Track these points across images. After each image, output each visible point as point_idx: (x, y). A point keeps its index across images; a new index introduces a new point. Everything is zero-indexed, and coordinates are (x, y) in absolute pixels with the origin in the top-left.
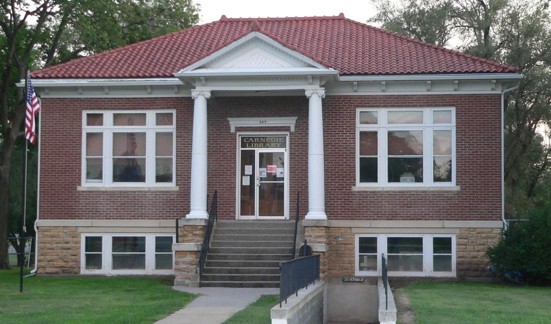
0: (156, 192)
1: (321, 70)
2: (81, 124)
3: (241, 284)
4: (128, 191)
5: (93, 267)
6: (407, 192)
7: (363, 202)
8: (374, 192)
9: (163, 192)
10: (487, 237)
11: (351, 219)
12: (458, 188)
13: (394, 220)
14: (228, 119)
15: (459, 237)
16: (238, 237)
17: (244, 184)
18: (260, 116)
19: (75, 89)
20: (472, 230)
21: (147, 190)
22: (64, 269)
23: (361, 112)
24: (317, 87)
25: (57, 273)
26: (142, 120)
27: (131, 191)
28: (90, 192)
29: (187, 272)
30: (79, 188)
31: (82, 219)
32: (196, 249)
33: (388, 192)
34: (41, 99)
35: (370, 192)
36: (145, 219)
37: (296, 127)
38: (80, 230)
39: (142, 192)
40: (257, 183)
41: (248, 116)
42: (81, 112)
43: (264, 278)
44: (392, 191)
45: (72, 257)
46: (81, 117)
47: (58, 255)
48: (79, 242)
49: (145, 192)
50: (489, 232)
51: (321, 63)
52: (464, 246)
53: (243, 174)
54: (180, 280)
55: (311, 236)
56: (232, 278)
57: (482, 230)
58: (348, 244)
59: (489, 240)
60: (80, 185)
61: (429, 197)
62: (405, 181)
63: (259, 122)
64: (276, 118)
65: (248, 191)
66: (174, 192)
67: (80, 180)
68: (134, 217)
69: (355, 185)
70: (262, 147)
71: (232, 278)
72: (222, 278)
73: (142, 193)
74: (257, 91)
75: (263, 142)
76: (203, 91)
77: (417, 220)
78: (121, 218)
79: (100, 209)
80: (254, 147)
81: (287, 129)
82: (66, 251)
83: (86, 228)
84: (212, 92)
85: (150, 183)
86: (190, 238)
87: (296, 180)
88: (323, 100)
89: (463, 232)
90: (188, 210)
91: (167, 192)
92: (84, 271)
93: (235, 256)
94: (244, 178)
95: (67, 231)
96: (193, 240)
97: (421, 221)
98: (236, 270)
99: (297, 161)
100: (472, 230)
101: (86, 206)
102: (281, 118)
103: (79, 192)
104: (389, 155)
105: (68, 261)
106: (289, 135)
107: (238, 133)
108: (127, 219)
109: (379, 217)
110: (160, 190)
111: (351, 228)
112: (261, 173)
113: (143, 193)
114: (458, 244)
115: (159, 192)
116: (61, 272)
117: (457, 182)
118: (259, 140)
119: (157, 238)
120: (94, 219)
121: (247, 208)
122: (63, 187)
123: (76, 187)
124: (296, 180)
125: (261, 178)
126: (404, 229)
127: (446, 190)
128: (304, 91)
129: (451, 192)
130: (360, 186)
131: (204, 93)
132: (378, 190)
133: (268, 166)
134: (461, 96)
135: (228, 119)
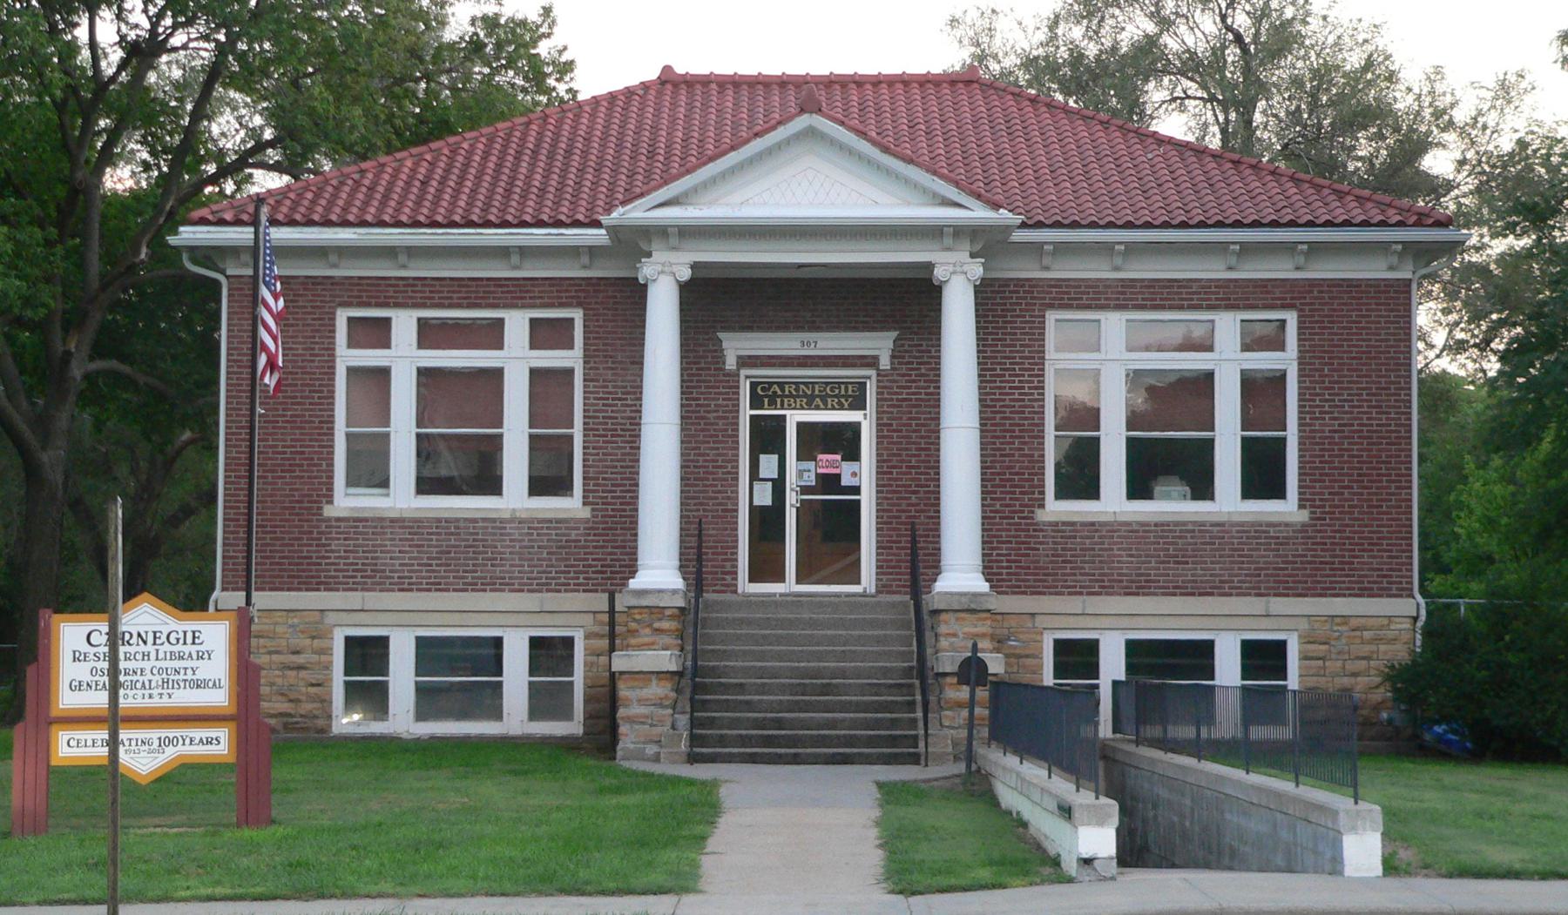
0: (532, 520)
1: (979, 213)
4: (457, 520)
6: (1177, 524)
8: (1093, 524)
9: (550, 521)
10: (1377, 640)
11: (1033, 593)
13: (1144, 594)
14: (721, 335)
15: (1307, 639)
16: (764, 636)
17: (756, 503)
18: (799, 328)
20: (1338, 620)
21: (507, 516)
23: (1057, 320)
24: (964, 256)
30: (329, 511)
32: (673, 668)
34: (227, 277)
35: (1083, 524)
37: (893, 357)
38: (331, 618)
39: (494, 520)
40: (791, 499)
43: (850, 741)
44: (1138, 523)
45: (312, 690)
48: (327, 651)
49: (502, 521)
50: (1381, 628)
51: (979, 197)
53: (754, 475)
55: (955, 635)
56: (769, 741)
57: (1363, 621)
58: (1027, 656)
59: (1383, 648)
60: (331, 502)
62: (1167, 497)
63: (798, 345)
65: (767, 522)
67: (331, 490)
69: (1042, 506)
71: (769, 741)
72: (744, 741)
73: (495, 524)
75: (805, 395)
76: (671, 264)
77: (1201, 594)
78: (437, 586)
80: (782, 408)
82: (294, 673)
83: (346, 614)
84: (695, 266)
86: (646, 640)
88: (978, 291)
91: (559, 521)
94: (757, 485)
100: (1338, 620)
103: (329, 519)
104: (1128, 430)
105: (298, 701)
106: (874, 378)
107: (743, 372)
109: (1106, 586)
110: (541, 516)
111: (1033, 615)
112: (800, 473)
114: (1304, 657)
116: (280, 727)
119: (419, 640)
121: (766, 566)
126: (1169, 619)
128: (929, 266)
129: (1287, 525)
130: (1056, 509)
131: (675, 269)
132: (1103, 519)
133: (820, 457)
134: (1313, 283)
135: (721, 335)
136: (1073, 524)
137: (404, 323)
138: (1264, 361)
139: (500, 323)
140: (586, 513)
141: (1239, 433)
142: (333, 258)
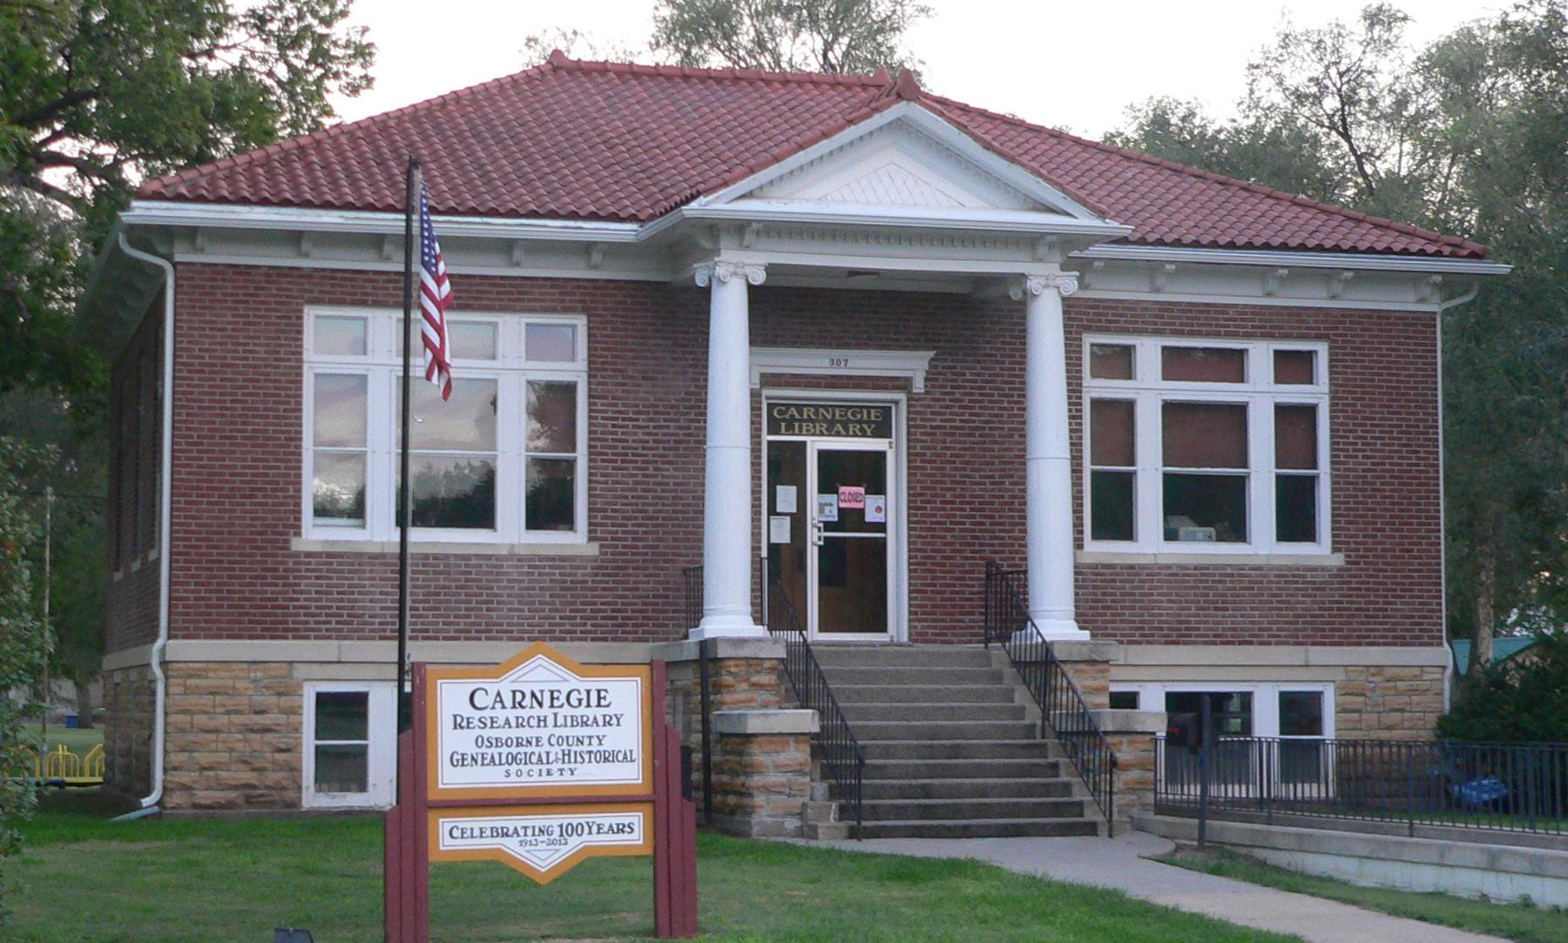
0: (531, 558)
2: (301, 346)
3: (966, 827)
4: (447, 556)
5: (338, 786)
6: (1216, 567)
7: (1104, 594)
8: (1132, 567)
9: (553, 559)
10: (1413, 691)
12: (1338, 560)
13: (1185, 643)
15: (1343, 691)
16: (858, 692)
19: (294, 238)
20: (1373, 670)
22: (253, 792)
24: (1054, 268)
25: (230, 805)
26: (1232, 366)
27: (455, 556)
28: (330, 555)
29: (789, 795)
30: (297, 545)
31: (308, 638)
32: (816, 729)
33: (1168, 567)
34: (175, 265)
35: (1123, 567)
36: (501, 639)
37: (926, 379)
38: (300, 672)
39: (489, 557)
40: (814, 537)
41: (785, 344)
42: (301, 311)
43: (1014, 811)
45: (279, 756)
46: (301, 325)
47: (232, 750)
48: (296, 710)
49: (498, 558)
50: (1415, 678)
51: (1084, 203)
52: (1356, 715)
54: (769, 820)
56: (926, 812)
59: (1415, 699)
60: (298, 534)
61: (1270, 582)
62: (1192, 538)
63: (827, 362)
64: (813, 351)
66: (581, 558)
67: (298, 519)
68: (466, 634)
70: (822, 434)
71: (926, 812)
72: (900, 812)
73: (491, 562)
74: (853, 273)
75: (825, 420)
76: (744, 265)
77: (1240, 643)
79: (363, 608)
80: (800, 434)
81: (903, 384)
82: (258, 736)
84: (771, 269)
85: (1263, 541)
86: (743, 696)
87: (929, 530)
89: (1353, 676)
90: (695, 610)
91: (563, 559)
92: (313, 798)
93: (889, 746)
94: (775, 521)
95: (259, 674)
96: (751, 700)
97: (1251, 648)
98: (923, 787)
99: (930, 475)
100: (1373, 670)
101: (320, 600)
102: (914, 353)
103: (297, 555)
104: (1165, 465)
105: (265, 769)
108: (445, 639)
110: (543, 552)
112: (822, 507)
113: (494, 562)
114: (1342, 710)
115: (541, 558)
116: (240, 801)
117: (1334, 542)
118: (816, 413)
120: (345, 638)
122: (246, 541)
123: (287, 541)
124: (929, 530)
125: (826, 523)
126: (1205, 669)
127: (1311, 563)
129: (1323, 569)
131: (748, 270)
132: (1142, 561)
133: (842, 489)
134: (1345, 313)
136: (1113, 566)
137: (1148, 352)
138: (1295, 394)
139: (1241, 354)
140: (593, 550)
141: (1161, 469)
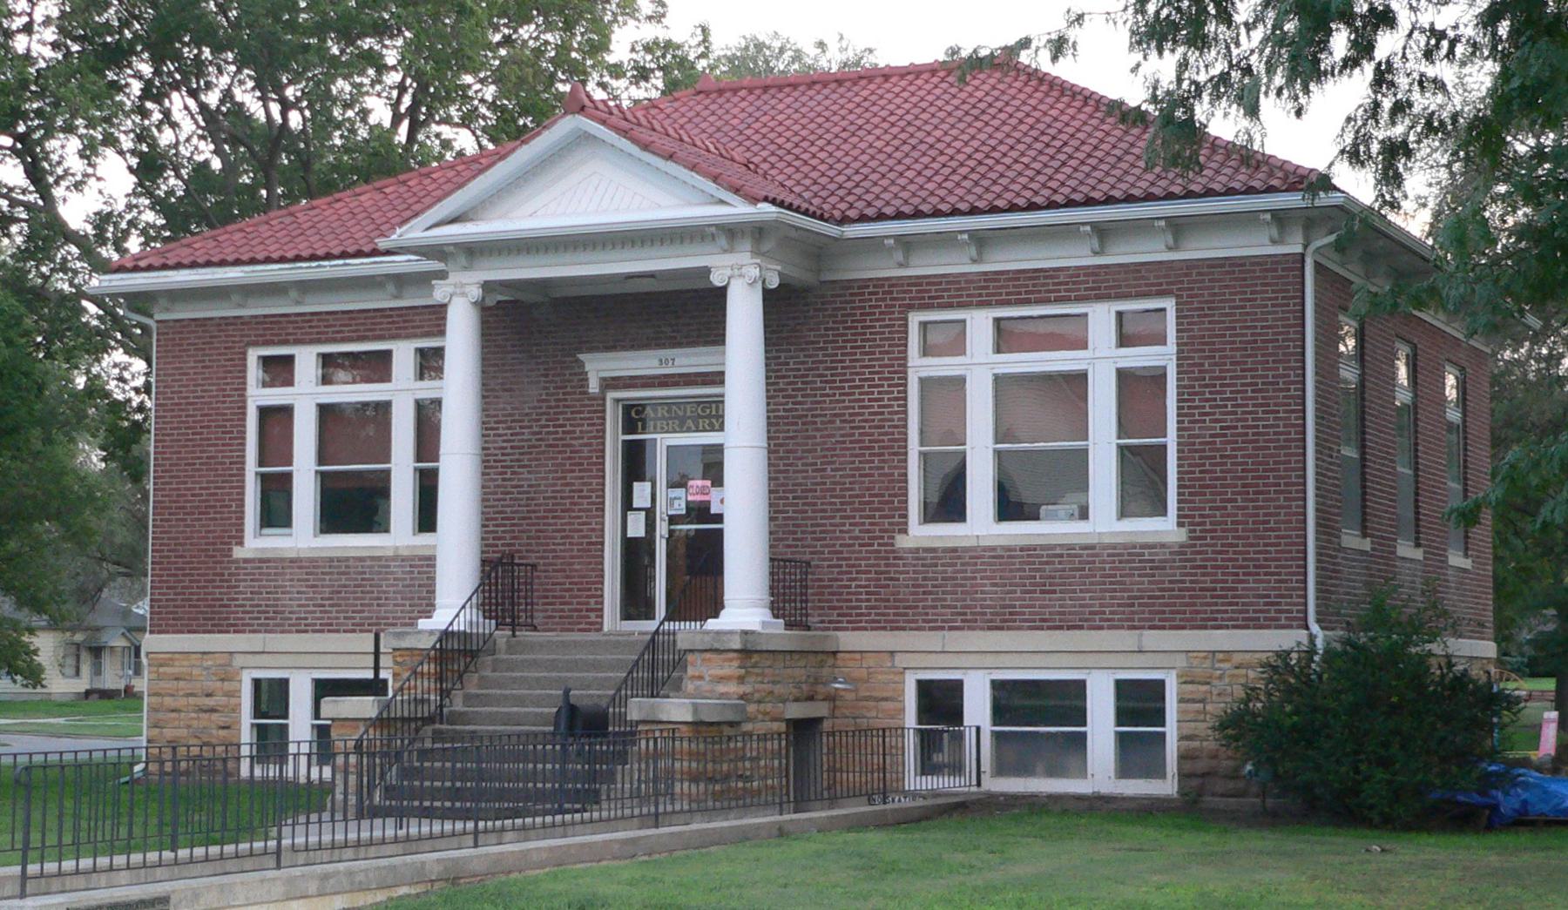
0: (412, 558)
1: (739, 210)
4: (347, 559)
6: (1043, 547)
8: (954, 550)
11: (892, 629)
13: (1009, 628)
14: (581, 357)
15: (1186, 679)
16: (538, 679)
17: (630, 534)
18: (660, 345)
20: (1221, 656)
21: (390, 553)
28: (261, 561)
30: (238, 553)
31: (243, 632)
33: (993, 549)
35: (945, 550)
38: (239, 661)
39: (379, 558)
40: (662, 529)
44: (1003, 548)
45: (222, 733)
47: (189, 727)
48: (235, 694)
49: (387, 559)
53: (628, 505)
55: (701, 678)
57: (1248, 656)
58: (886, 699)
60: (241, 543)
61: (1104, 562)
62: (1054, 517)
63: (656, 363)
65: (636, 554)
69: (905, 532)
73: (379, 562)
74: (630, 277)
76: (463, 285)
77: (1069, 628)
78: (329, 628)
83: (253, 655)
84: (487, 286)
88: (770, 297)
89: (1195, 663)
94: (631, 516)
97: (1077, 632)
100: (1221, 656)
103: (237, 561)
107: (611, 395)
109: (969, 620)
111: (892, 653)
121: (636, 602)
123: (230, 550)
126: (1037, 656)
128: (706, 271)
129: (1163, 546)
130: (921, 533)
134: (1190, 265)
135: (581, 357)
136: (934, 550)
138: (1140, 357)
142: (293, 294)
